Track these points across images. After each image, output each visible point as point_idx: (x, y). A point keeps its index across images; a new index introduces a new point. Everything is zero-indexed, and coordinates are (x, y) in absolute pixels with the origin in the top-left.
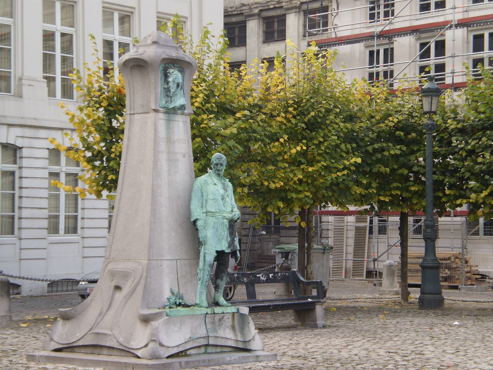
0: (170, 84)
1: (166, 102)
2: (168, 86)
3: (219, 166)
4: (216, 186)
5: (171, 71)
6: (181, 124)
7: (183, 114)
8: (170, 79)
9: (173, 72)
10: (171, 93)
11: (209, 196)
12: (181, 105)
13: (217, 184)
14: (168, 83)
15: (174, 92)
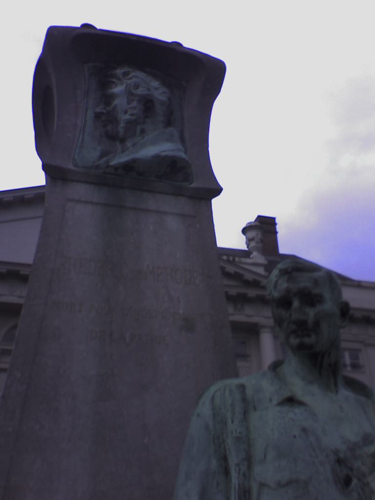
0: (116, 102)
1: (103, 154)
2: (110, 108)
3: (296, 304)
4: (298, 410)
5: (119, 72)
6: (173, 223)
7: (177, 193)
8: (118, 89)
9: (125, 74)
10: (122, 125)
11: (257, 469)
12: (158, 159)
13: (306, 399)
14: (107, 99)
15: (131, 125)
